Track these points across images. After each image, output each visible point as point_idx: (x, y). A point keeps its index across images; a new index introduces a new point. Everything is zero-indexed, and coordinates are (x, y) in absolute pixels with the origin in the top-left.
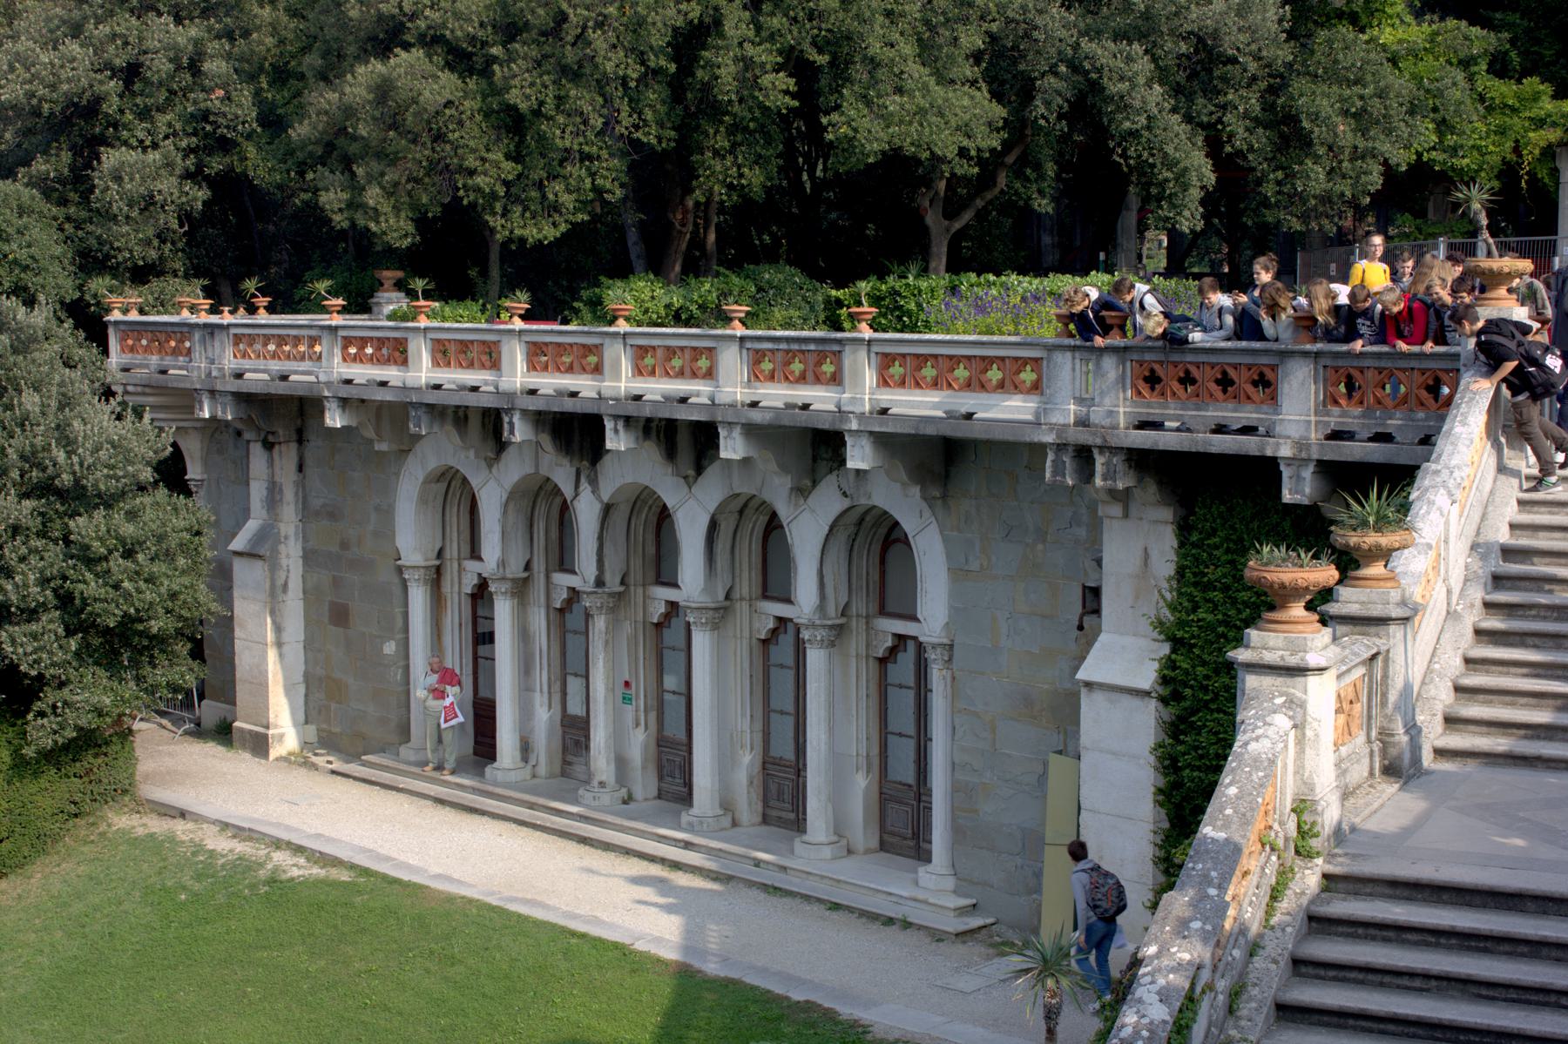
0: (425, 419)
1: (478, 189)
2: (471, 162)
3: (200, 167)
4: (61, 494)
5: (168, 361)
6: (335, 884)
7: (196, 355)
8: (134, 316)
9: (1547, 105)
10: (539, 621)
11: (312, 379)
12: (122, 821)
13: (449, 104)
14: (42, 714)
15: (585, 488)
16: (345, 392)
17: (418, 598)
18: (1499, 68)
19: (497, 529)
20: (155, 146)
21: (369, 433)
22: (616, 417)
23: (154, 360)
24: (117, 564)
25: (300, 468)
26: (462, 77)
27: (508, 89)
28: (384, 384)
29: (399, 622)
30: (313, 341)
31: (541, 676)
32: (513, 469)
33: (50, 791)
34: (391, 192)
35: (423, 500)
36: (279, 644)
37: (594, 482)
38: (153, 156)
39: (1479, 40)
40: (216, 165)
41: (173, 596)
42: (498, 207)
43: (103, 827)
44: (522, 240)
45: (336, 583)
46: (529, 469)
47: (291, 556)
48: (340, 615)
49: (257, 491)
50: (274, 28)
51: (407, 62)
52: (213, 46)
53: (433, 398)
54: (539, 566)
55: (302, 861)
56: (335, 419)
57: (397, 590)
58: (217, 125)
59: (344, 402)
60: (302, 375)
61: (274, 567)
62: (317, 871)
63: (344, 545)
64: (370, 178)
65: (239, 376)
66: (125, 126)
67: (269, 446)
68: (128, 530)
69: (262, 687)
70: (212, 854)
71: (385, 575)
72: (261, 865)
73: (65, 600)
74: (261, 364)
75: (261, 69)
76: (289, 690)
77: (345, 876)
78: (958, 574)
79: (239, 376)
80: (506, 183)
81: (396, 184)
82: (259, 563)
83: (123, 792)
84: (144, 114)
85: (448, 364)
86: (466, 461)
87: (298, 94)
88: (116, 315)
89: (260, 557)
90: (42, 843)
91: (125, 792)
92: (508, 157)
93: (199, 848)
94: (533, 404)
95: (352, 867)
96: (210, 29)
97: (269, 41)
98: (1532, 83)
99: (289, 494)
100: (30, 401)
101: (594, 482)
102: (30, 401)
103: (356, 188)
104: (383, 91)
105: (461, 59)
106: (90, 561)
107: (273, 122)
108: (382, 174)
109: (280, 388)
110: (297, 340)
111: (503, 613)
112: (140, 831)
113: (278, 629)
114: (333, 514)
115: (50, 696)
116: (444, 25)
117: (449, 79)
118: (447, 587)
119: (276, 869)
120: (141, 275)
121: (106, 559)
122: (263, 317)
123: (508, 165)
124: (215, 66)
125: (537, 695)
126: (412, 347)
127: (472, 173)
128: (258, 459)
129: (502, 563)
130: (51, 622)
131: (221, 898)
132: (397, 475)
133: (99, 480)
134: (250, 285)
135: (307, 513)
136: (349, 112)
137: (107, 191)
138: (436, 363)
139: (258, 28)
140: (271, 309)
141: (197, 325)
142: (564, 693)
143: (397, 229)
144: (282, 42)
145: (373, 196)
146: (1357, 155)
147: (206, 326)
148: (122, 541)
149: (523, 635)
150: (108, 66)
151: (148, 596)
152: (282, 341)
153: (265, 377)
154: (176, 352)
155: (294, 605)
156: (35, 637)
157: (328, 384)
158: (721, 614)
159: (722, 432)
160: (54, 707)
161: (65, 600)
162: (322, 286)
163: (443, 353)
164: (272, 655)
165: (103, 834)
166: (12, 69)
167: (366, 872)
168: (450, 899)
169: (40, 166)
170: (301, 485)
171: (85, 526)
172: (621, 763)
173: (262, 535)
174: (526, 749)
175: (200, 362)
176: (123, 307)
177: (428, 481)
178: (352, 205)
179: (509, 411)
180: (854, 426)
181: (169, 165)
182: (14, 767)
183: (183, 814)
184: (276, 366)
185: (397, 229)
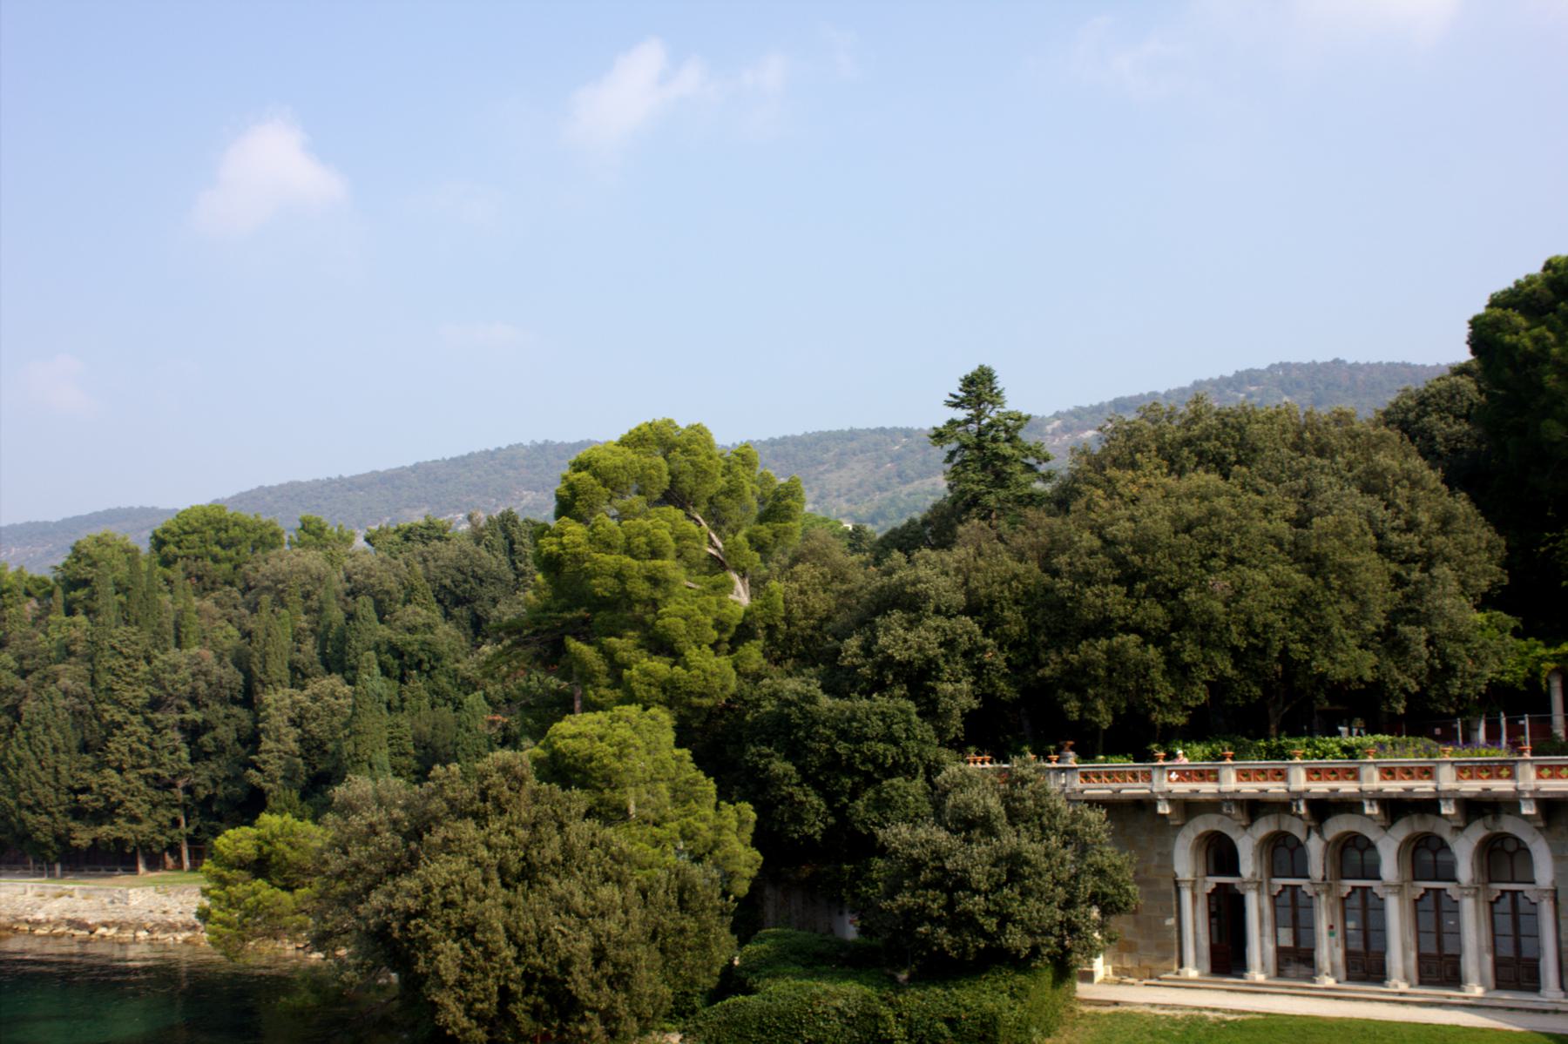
9: (1541, 651)
10: (1266, 902)
11: (1147, 791)
15: (1314, 838)
18: (1516, 633)
22: (1371, 800)
29: (1175, 909)
31: (1268, 929)
39: (1512, 622)
54: (1265, 876)
56: (1164, 809)
57: (1173, 892)
64: (1096, 695)
65: (1082, 791)
77: (1261, 1017)
78: (1558, 858)
85: (1249, 780)
94: (1307, 796)
98: (1532, 640)
101: (1320, 832)
116: (1144, 622)
129: (1254, 874)
132: (1176, 837)
142: (1277, 936)
146: (1473, 676)
149: (1261, 911)
157: (1161, 793)
158: (1399, 889)
159: (1442, 803)
162: (1154, 746)
167: (1268, 1014)
172: (1333, 965)
177: (1199, 837)
179: (1297, 800)
180: (1527, 795)
183: (1116, 1003)
184: (1115, 786)
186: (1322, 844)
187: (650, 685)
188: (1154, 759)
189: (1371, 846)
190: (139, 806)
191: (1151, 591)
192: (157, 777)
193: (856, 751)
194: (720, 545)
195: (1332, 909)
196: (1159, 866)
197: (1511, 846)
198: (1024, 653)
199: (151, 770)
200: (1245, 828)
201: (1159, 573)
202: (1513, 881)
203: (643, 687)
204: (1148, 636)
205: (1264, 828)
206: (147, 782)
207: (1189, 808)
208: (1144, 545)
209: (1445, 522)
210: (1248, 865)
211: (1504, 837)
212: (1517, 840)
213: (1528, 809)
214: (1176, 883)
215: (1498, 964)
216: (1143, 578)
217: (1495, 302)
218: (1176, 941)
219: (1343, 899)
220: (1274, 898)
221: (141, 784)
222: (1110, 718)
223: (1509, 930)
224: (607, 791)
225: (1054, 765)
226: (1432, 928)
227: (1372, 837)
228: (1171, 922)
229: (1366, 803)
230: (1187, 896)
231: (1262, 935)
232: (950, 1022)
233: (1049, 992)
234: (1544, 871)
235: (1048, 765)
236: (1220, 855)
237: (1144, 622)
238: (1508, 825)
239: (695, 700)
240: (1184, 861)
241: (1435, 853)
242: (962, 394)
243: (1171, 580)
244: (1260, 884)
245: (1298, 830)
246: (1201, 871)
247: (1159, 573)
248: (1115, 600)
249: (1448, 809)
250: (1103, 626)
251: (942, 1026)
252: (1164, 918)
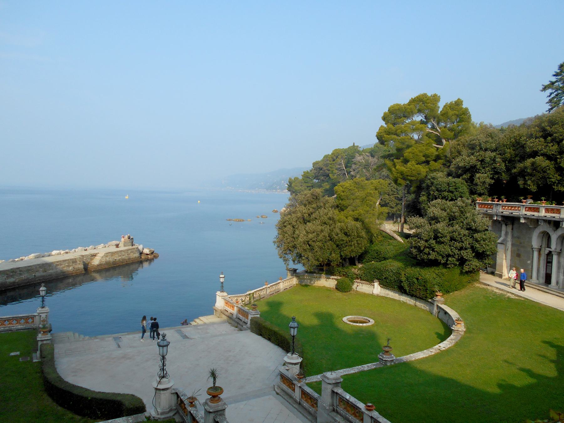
0: (542, 222)
1: (551, 181)
2: (551, 176)
3: (493, 176)
4: (472, 230)
5: (488, 209)
6: (521, 300)
7: (494, 209)
8: (481, 202)
11: (518, 214)
12: (477, 285)
13: (548, 166)
14: (466, 265)
16: (525, 216)
17: (536, 254)
19: (555, 243)
20: (485, 173)
21: (529, 224)
23: (485, 209)
24: (482, 242)
25: (512, 229)
26: (551, 161)
27: (560, 163)
28: (534, 215)
29: (531, 258)
30: (519, 207)
33: (465, 278)
34: (532, 182)
35: (539, 236)
36: (506, 259)
38: (486, 175)
40: (497, 176)
41: (491, 248)
42: (556, 184)
43: (474, 285)
44: (560, 191)
45: (518, 250)
47: (509, 245)
48: (519, 255)
49: (503, 233)
50: (510, 153)
51: (539, 159)
52: (497, 156)
53: (545, 218)
55: (513, 296)
56: (522, 221)
57: (531, 252)
58: (497, 170)
59: (525, 218)
60: (516, 213)
61: (506, 246)
62: (517, 297)
63: (521, 243)
64: (529, 179)
65: (502, 213)
66: (480, 170)
67: (506, 225)
68: (484, 237)
69: (502, 266)
70: (496, 292)
71: (530, 249)
72: (506, 295)
73: (472, 247)
74: (507, 211)
75: (507, 160)
76: (507, 267)
77: (523, 299)
79: (502, 213)
80: (557, 180)
81: (534, 180)
82: (503, 245)
83: (477, 280)
84: (484, 168)
85: (549, 212)
86: (550, 230)
87: (514, 164)
88: (478, 201)
89: (503, 244)
90: (464, 286)
91: (477, 280)
92: (559, 175)
93: (493, 291)
95: (524, 298)
96: (497, 153)
97: (509, 155)
99: (510, 233)
100: (468, 215)
102: (468, 215)
103: (525, 181)
104: (533, 164)
105: (549, 157)
106: (477, 241)
107: (508, 170)
108: (531, 179)
109: (511, 215)
110: (516, 207)
111: (555, 258)
112: (481, 287)
113: (506, 257)
114: (518, 238)
115: (467, 263)
117: (547, 161)
118: (542, 252)
119: (509, 296)
120: (480, 195)
121: (480, 241)
122: (505, 203)
123: (559, 177)
124: (498, 160)
125: (561, 274)
126: (540, 209)
127: (550, 178)
128: (504, 227)
129: (556, 249)
130: (469, 251)
131: (498, 299)
133: (480, 228)
134: (503, 197)
135: (513, 237)
136: (526, 168)
137: (476, 180)
138: (546, 212)
139: (507, 153)
140: (506, 201)
141: (495, 204)
143: (533, 188)
144: (511, 155)
145: (529, 182)
147: (496, 204)
148: (483, 238)
150: (478, 160)
151: (487, 248)
152: (512, 207)
153: (508, 213)
154: (490, 208)
155: (509, 253)
156: (466, 252)
157: (522, 215)
160: (469, 264)
161: (472, 247)
163: (547, 210)
164: (504, 261)
165: (474, 287)
166: (461, 161)
167: (527, 299)
168: (546, 306)
169: (464, 176)
170: (512, 232)
171: (476, 235)
173: (504, 240)
174: (557, 283)
175: (494, 210)
176: (479, 200)
177: (540, 233)
178: (524, 184)
181: (488, 176)
182: (460, 273)
183: (489, 285)
184: (511, 211)
185: (533, 188)
187: (398, 173)
190: (393, 204)
191: (552, 141)
192: (398, 198)
193: (440, 195)
194: (439, 130)
198: (510, 163)
199: (396, 195)
200: (555, 231)
201: (556, 133)
203: (396, 173)
206: (395, 199)
207: (536, 222)
216: (551, 135)
218: (530, 269)
221: (394, 199)
222: (535, 187)
224: (340, 201)
225: (496, 203)
228: (529, 262)
232: (417, 279)
233: (458, 276)
235: (494, 203)
237: (547, 152)
239: (409, 178)
240: (535, 242)
242: (559, 71)
243: (561, 135)
246: (543, 246)
247: (556, 133)
250: (534, 154)
251: (415, 280)
252: (528, 260)
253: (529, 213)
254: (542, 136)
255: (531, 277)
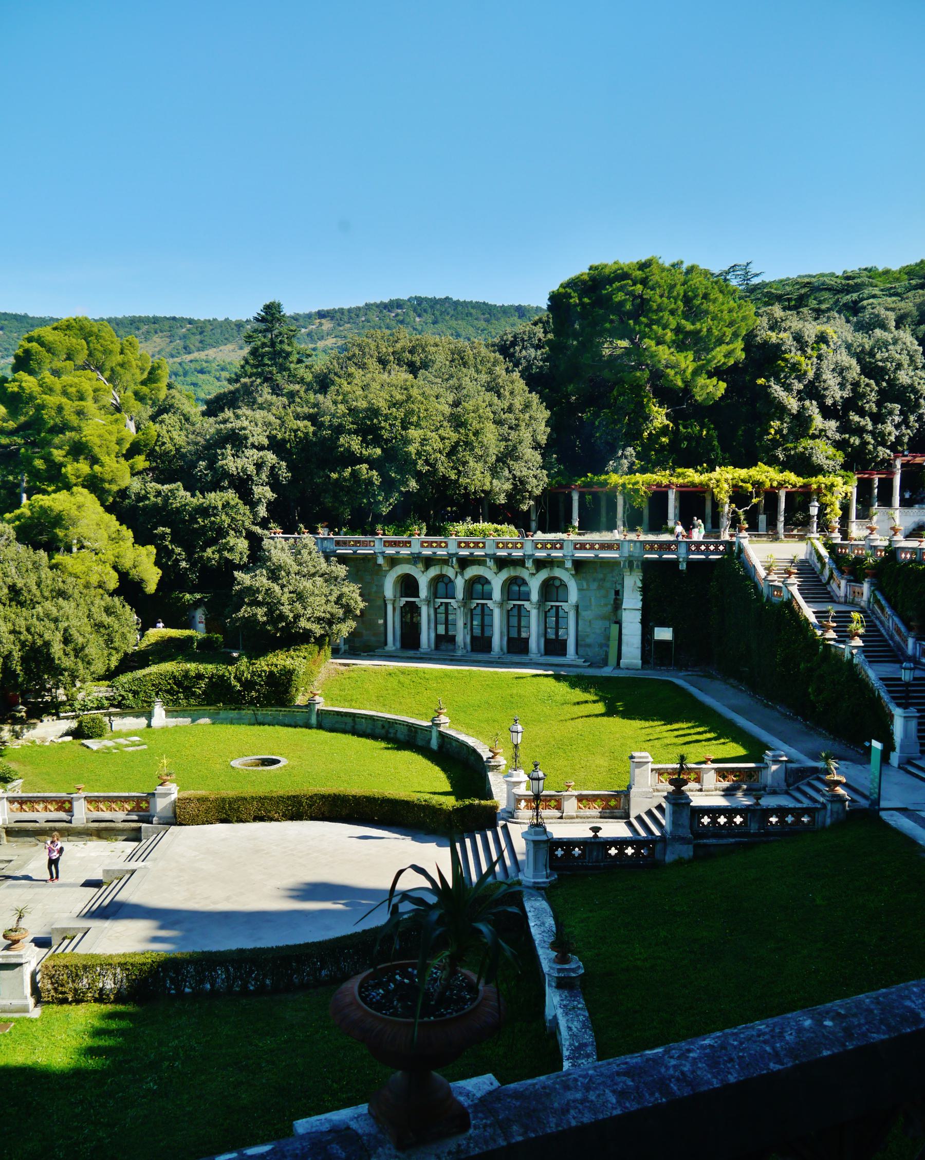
10: (432, 612)
15: (459, 577)
31: (432, 625)
32: (433, 572)
37: (462, 574)
46: (438, 572)
56: (380, 561)
71: (380, 602)
78: (580, 590)
101: (462, 574)
104: (354, 474)
118: (396, 605)
149: (429, 616)
172: (465, 644)
186: (463, 581)
188: (377, 534)
189: (487, 582)
195: (466, 615)
196: (376, 592)
197: (557, 583)
200: (423, 572)
202: (557, 601)
204: (373, 463)
205: (433, 572)
207: (393, 561)
208: (374, 412)
209: (527, 406)
210: (423, 592)
211: (554, 578)
212: (561, 580)
213: (569, 564)
214: (385, 601)
215: (547, 642)
217: (562, 286)
219: (472, 610)
220: (436, 609)
223: (553, 625)
226: (516, 625)
227: (489, 577)
228: (381, 622)
229: (488, 560)
230: (390, 608)
231: (429, 628)
234: (573, 596)
236: (408, 585)
238: (558, 572)
241: (519, 586)
244: (429, 602)
245: (450, 572)
246: (398, 595)
248: (355, 443)
249: (529, 564)
253: (391, 551)
254: (356, 432)
255: (386, 644)
